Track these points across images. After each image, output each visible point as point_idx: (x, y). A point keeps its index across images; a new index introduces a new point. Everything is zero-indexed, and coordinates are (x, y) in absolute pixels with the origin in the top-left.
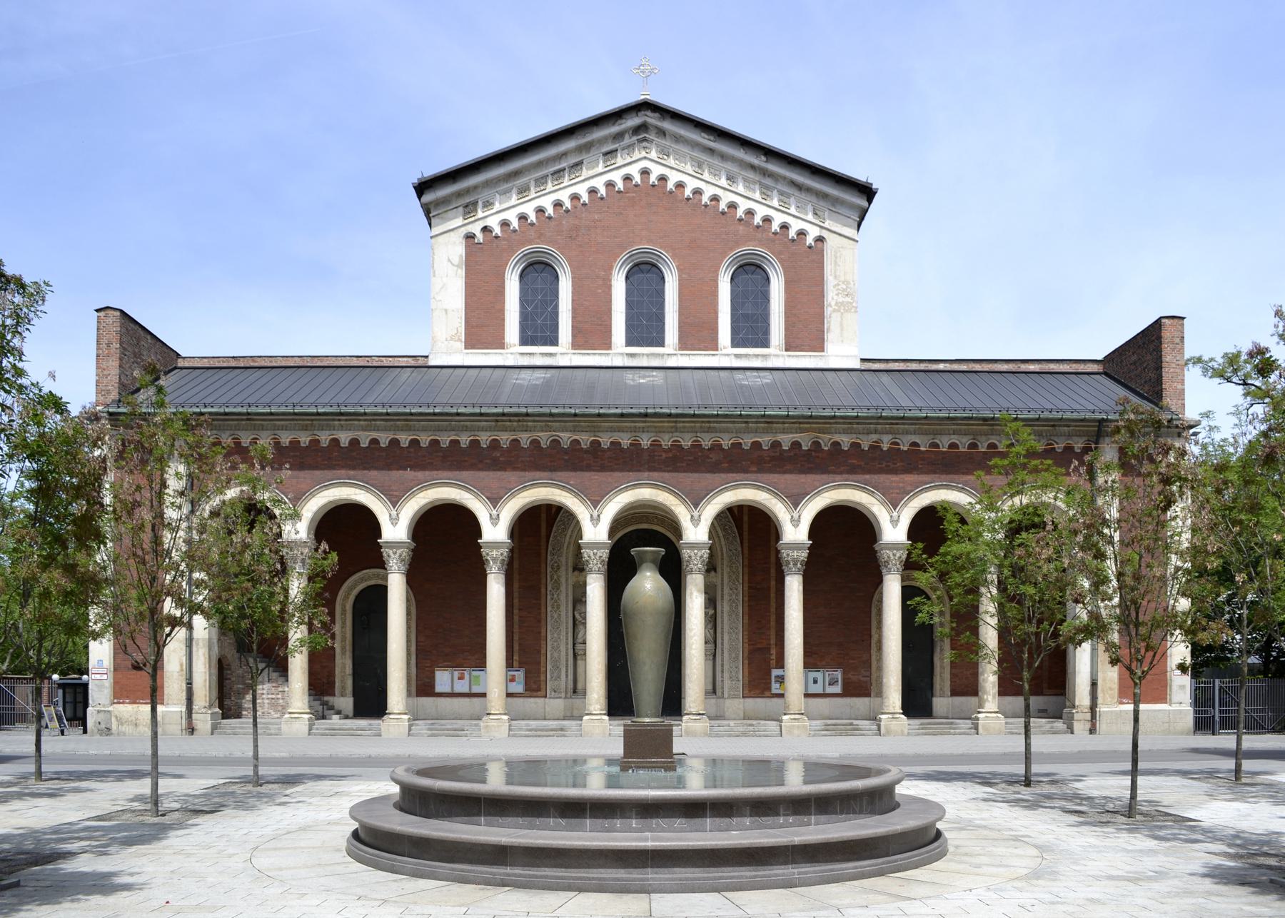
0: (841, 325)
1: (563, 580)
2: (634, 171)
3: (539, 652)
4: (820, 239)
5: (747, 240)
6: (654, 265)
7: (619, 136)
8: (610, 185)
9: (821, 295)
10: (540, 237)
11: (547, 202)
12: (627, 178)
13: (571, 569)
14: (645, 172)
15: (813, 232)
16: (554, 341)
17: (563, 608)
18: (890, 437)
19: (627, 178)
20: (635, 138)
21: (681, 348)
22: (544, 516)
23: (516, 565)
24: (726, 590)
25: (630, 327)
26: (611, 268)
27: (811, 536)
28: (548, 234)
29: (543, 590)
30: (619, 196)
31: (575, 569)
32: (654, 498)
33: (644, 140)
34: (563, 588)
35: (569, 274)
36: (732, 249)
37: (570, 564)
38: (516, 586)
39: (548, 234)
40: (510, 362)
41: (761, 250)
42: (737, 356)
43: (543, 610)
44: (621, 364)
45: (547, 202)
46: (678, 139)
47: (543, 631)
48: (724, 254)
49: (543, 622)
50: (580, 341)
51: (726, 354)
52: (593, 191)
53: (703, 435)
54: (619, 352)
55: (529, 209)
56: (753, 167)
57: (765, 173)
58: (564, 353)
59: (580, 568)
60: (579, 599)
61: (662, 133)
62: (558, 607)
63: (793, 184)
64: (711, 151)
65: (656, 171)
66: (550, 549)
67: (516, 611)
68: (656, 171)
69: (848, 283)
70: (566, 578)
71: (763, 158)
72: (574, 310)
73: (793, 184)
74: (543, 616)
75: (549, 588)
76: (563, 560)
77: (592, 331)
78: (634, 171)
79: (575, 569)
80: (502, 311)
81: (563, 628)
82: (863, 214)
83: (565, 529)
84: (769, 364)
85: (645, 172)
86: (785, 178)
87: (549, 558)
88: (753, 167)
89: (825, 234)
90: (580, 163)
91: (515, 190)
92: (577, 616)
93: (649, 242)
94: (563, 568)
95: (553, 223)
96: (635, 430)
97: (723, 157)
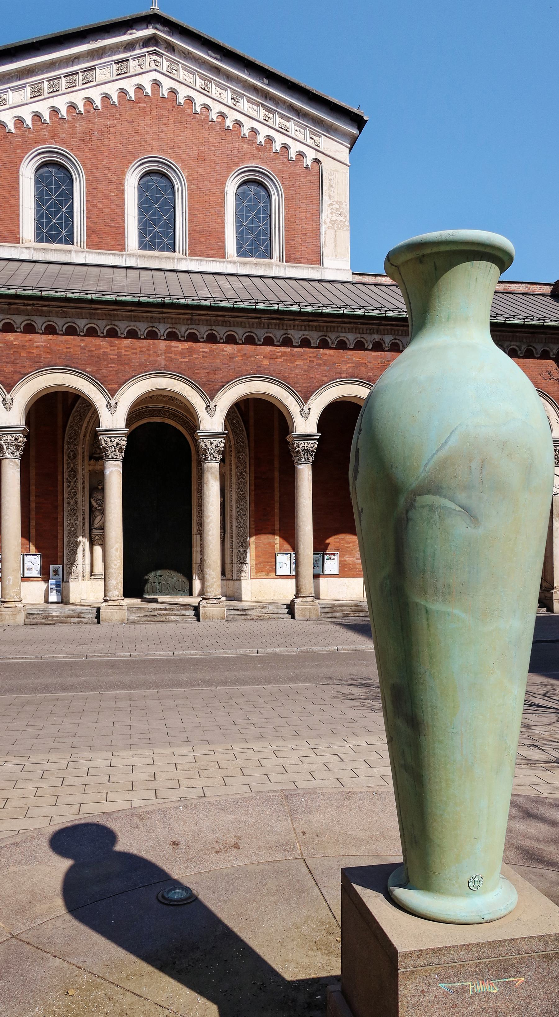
0: (335, 242)
1: (80, 469)
2: (146, 81)
3: (56, 537)
4: (317, 161)
5: (252, 157)
6: (164, 175)
7: (129, 46)
8: (123, 92)
9: (319, 212)
10: (54, 136)
11: (61, 103)
12: (139, 88)
13: (87, 458)
14: (156, 84)
15: (311, 155)
16: (70, 240)
17: (80, 495)
18: (391, 337)
19: (139, 88)
20: (145, 50)
21: (191, 254)
22: (60, 407)
23: (33, 453)
24: (234, 480)
25: (143, 232)
26: (124, 173)
27: (319, 429)
28: (62, 136)
29: (60, 478)
30: (130, 105)
31: (91, 458)
32: (170, 388)
33: (156, 53)
34: (80, 476)
35: (83, 176)
36: (237, 166)
37: (86, 454)
38: (33, 473)
39: (62, 136)
40: (25, 256)
41: (265, 168)
42: (243, 264)
43: (60, 497)
44: (134, 265)
45: (61, 103)
46: (187, 56)
47: (60, 517)
48: (230, 169)
49: (60, 509)
50: (95, 241)
51: (232, 263)
52: (106, 97)
53: (218, 328)
54: (132, 253)
55: (43, 108)
56: (256, 90)
57: (266, 96)
58: (78, 253)
59: (97, 455)
60: (98, 485)
61: (171, 48)
62: (75, 493)
63: (292, 108)
64: (217, 70)
65: (167, 84)
66: (66, 438)
67: (33, 498)
68: (167, 84)
69: (341, 203)
70: (83, 468)
71: (266, 81)
72: (89, 211)
73: (292, 108)
74: (60, 502)
75: (66, 476)
76: (80, 449)
77: (106, 234)
78: (146, 81)
79: (91, 458)
80: (16, 206)
81: (80, 514)
82: (353, 141)
83: (81, 420)
84: (272, 274)
85: (156, 84)
86: (284, 102)
87: (66, 447)
88: (256, 90)
89: (320, 157)
90: (93, 68)
91: (28, 89)
92: (94, 503)
93: (160, 150)
94: (80, 457)
95: (66, 126)
96: (152, 320)
97: (229, 77)
